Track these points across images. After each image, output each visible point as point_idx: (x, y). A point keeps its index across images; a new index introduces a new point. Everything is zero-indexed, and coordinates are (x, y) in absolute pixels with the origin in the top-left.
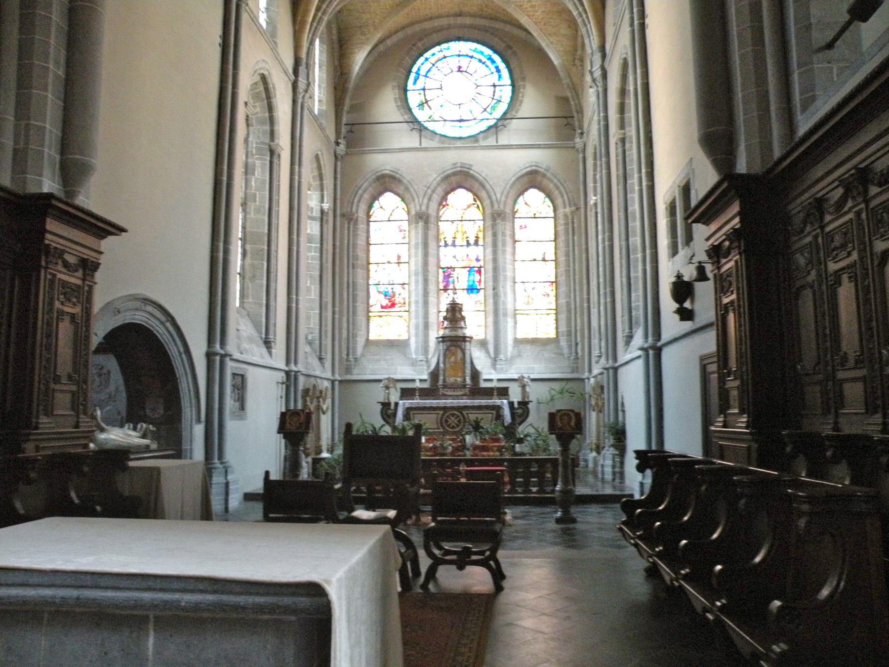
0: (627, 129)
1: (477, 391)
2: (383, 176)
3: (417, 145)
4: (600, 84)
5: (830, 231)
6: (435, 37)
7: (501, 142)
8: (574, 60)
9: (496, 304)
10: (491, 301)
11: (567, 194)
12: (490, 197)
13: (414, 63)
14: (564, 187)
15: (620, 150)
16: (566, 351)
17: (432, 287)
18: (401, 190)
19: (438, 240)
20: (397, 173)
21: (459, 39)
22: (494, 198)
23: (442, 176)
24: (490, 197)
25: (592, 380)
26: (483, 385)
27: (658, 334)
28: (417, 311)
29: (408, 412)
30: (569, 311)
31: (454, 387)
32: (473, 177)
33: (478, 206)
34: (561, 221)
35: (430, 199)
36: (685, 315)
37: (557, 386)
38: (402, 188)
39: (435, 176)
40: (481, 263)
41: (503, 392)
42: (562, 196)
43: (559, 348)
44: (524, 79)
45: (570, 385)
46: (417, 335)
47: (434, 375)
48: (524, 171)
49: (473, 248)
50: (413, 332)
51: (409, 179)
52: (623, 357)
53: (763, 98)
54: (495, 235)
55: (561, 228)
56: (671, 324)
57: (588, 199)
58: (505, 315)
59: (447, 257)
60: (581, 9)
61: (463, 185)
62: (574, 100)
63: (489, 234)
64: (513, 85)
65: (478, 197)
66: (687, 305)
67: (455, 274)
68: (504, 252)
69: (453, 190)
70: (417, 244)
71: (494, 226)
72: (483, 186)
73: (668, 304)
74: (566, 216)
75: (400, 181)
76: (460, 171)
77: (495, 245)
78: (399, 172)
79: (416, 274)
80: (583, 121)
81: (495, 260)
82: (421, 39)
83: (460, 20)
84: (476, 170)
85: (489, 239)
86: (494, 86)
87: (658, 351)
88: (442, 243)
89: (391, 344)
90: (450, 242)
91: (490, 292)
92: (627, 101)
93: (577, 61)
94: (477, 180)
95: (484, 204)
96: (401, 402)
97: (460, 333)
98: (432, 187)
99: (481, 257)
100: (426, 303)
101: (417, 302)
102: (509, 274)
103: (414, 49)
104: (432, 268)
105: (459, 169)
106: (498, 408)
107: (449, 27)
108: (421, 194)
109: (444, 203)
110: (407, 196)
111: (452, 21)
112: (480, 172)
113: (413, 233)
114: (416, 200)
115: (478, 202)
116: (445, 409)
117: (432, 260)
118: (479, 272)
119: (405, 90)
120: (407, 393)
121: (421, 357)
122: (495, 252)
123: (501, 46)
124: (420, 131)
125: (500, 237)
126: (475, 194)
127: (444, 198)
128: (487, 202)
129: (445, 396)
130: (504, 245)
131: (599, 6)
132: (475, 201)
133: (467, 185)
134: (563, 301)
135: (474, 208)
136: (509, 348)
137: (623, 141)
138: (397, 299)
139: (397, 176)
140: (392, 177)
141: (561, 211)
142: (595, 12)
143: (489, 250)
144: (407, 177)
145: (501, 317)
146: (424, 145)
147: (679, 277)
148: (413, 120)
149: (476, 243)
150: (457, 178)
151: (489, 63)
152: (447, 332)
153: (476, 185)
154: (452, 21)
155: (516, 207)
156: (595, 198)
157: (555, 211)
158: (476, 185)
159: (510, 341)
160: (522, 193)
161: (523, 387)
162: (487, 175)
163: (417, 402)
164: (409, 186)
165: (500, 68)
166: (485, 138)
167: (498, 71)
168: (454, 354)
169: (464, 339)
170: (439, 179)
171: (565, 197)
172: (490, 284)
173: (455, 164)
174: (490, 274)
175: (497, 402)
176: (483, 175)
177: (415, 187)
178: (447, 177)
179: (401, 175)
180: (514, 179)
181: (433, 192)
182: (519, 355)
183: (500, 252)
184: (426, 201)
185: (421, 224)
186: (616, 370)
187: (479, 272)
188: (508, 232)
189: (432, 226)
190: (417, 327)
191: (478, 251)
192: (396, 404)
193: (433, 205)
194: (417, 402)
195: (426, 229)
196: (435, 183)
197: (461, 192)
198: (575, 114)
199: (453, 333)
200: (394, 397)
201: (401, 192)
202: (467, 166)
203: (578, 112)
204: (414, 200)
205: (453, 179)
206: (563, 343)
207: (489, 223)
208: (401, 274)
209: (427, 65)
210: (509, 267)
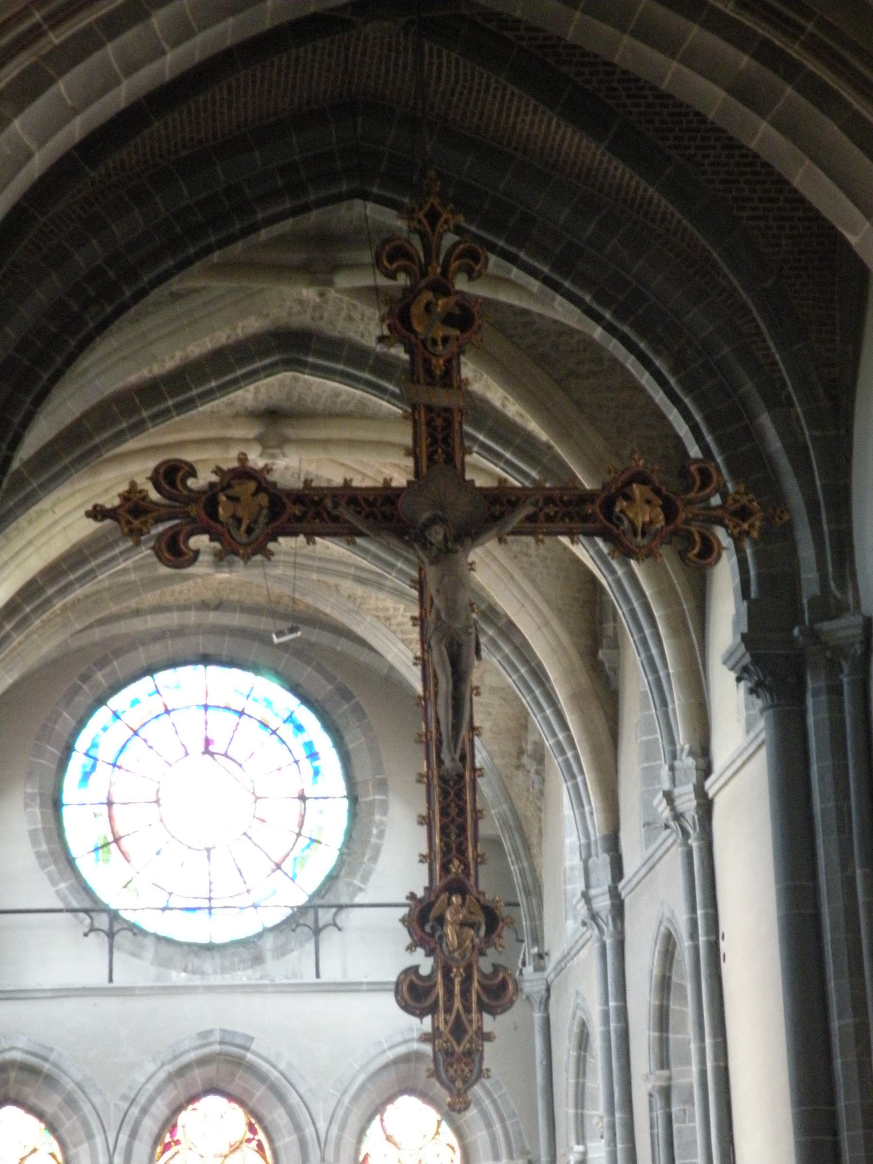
0: (675, 1068)
3: (101, 980)
4: (609, 929)
6: (141, 656)
7: (331, 973)
8: (521, 752)
11: (502, 1120)
12: (298, 1128)
13: (81, 723)
14: (494, 1102)
15: (659, 1113)
18: (51, 1104)
20: (46, 1059)
21: (206, 659)
22: (309, 1131)
23: (170, 1068)
24: (298, 1128)
32: (252, 1069)
33: (260, 1146)
35: (133, 1134)
38: (57, 1099)
39: (150, 1067)
42: (489, 1125)
44: (382, 785)
48: (391, 1055)
51: (78, 1077)
57: (560, 1151)
60: (561, 736)
61: (222, 1085)
62: (518, 858)
64: (353, 798)
65: (260, 1120)
69: (193, 1099)
72: (281, 1098)
75: (50, 1081)
76: (220, 1054)
78: (53, 1057)
80: (541, 918)
82: (103, 663)
83: (212, 617)
84: (260, 1051)
86: (302, 798)
92: (674, 1006)
93: (525, 760)
94: (263, 1078)
95: (279, 1144)
98: (142, 1100)
103: (86, 687)
105: (217, 1048)
107: (180, 632)
109: (167, 1139)
110: (69, 1123)
111: (192, 617)
112: (272, 1058)
114: (99, 1140)
115: (261, 1136)
119: (57, 804)
123: (323, 689)
124: (111, 935)
126: (251, 1112)
127: (169, 1124)
128: (287, 1140)
131: (604, 738)
132: (252, 1129)
133: (231, 1089)
135: (249, 1151)
137: (666, 1093)
139: (47, 1067)
140: (32, 1071)
142: (596, 752)
146: (119, 980)
148: (87, 904)
150: (210, 1071)
151: (286, 731)
154: (192, 617)
155: (364, 1149)
156: (580, 1148)
158: (260, 1091)
160: (378, 1109)
162: (290, 1065)
164: (78, 1095)
165: (317, 748)
166: (281, 952)
167: (313, 756)
170: (162, 1075)
171: (498, 1127)
173: (205, 1034)
176: (282, 1066)
177: (97, 1100)
178: (182, 1071)
179: (56, 1065)
180: (362, 1077)
181: (144, 1111)
184: (124, 1138)
196: (150, 1087)
197: (213, 1103)
198: (521, 899)
201: (49, 1109)
202: (238, 1041)
203: (527, 893)
204: (90, 1136)
205: (198, 1075)
209: (119, 733)
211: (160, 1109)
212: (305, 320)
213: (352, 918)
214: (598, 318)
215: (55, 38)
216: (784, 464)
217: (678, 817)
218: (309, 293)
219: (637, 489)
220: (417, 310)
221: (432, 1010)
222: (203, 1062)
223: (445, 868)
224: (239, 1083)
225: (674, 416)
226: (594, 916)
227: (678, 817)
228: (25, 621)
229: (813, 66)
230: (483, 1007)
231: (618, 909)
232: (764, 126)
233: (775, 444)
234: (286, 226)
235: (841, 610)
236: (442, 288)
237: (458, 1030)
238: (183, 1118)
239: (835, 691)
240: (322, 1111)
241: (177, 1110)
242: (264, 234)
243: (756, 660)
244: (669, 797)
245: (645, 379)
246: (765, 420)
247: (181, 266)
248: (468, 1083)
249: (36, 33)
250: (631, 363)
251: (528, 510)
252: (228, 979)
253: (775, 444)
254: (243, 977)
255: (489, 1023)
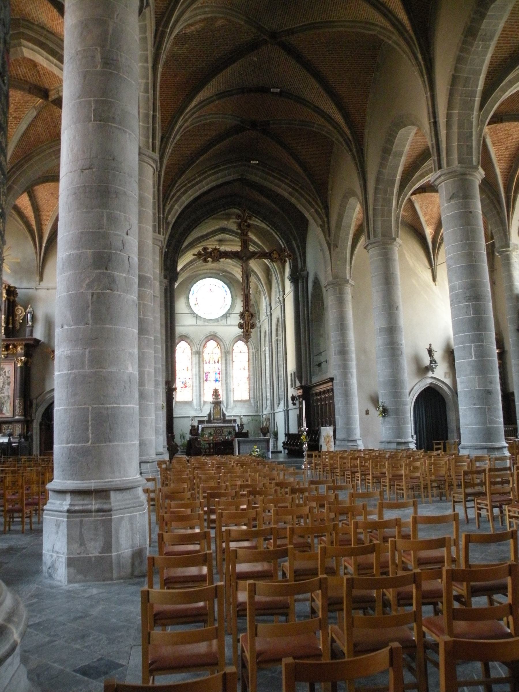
1: (225, 421)
2: (182, 336)
3: (195, 324)
5: (320, 393)
6: (201, 277)
7: (229, 323)
9: (227, 387)
10: (224, 386)
12: (224, 345)
16: (253, 405)
17: (202, 380)
18: (189, 341)
19: (203, 361)
21: (210, 277)
24: (224, 345)
25: (264, 416)
26: (227, 418)
27: (288, 406)
28: (196, 390)
29: (203, 429)
30: (254, 390)
31: (217, 419)
32: (217, 337)
34: (251, 355)
35: (200, 345)
36: (294, 404)
37: (250, 418)
40: (220, 370)
41: (235, 421)
43: (250, 403)
44: (236, 296)
45: (255, 417)
46: (196, 399)
47: (210, 415)
49: (217, 364)
50: (194, 398)
52: (277, 410)
53: (307, 371)
54: (226, 360)
55: (251, 357)
56: (291, 405)
58: (230, 391)
59: (207, 368)
63: (224, 359)
64: (232, 298)
66: (295, 402)
67: (209, 375)
68: (230, 367)
70: (196, 363)
71: (226, 356)
73: (290, 402)
74: (253, 353)
75: (188, 338)
77: (226, 363)
79: (196, 375)
81: (226, 370)
82: (195, 277)
83: (211, 271)
85: (224, 361)
87: (288, 411)
88: (205, 362)
89: (186, 403)
90: (207, 362)
91: (224, 382)
92: (279, 328)
94: (219, 338)
96: (200, 426)
97: (219, 400)
99: (220, 368)
100: (200, 387)
101: (196, 386)
102: (231, 375)
104: (202, 372)
106: (234, 427)
107: (206, 273)
108: (197, 343)
110: (191, 344)
111: (208, 271)
113: (194, 358)
116: (216, 427)
117: (201, 369)
118: (219, 374)
119: (188, 298)
120: (200, 422)
121: (198, 408)
122: (226, 367)
123: (228, 282)
125: (228, 361)
126: (217, 343)
127: (205, 344)
128: (222, 347)
129: (214, 423)
130: (230, 364)
134: (252, 385)
136: (232, 404)
138: (187, 385)
141: (251, 350)
142: (268, 291)
143: (224, 366)
144: (192, 336)
145: (229, 392)
146: (198, 324)
147: (293, 395)
149: (218, 362)
152: (214, 400)
153: (218, 340)
154: (208, 271)
157: (248, 349)
159: (232, 401)
160: (235, 343)
161: (241, 419)
163: (205, 425)
166: (222, 320)
168: (217, 408)
169: (220, 402)
172: (224, 379)
173: (210, 332)
174: (224, 375)
175: (233, 424)
178: (207, 337)
182: (236, 406)
183: (228, 367)
185: (197, 355)
186: (274, 414)
187: (219, 374)
188: (231, 359)
189: (201, 356)
190: (196, 396)
191: (219, 365)
192: (198, 427)
193: (202, 347)
194: (205, 425)
195: (199, 357)
197: (212, 341)
199: (216, 401)
200: (196, 424)
205: (210, 338)
206: (252, 401)
207: (223, 355)
208: (189, 374)
210: (231, 372)
211: (204, 342)
212: (225, 226)
213: (232, 315)
214: (269, 227)
215: (189, 185)
216: (296, 249)
217: (280, 301)
218: (226, 222)
219: (275, 252)
220: (242, 224)
221: (243, 328)
222: (210, 336)
223: (245, 308)
224: (215, 338)
225: (280, 241)
226: (267, 315)
227: (280, 301)
228: (184, 271)
229: (300, 190)
230: (251, 328)
231: (271, 314)
232: (293, 199)
233: (295, 246)
234: (223, 212)
235: (304, 271)
236: (246, 221)
237: (247, 331)
238: (208, 344)
239: (303, 282)
240: (227, 343)
241: (207, 342)
242: (220, 213)
243: (292, 278)
244: (279, 298)
245: (276, 236)
246: (294, 242)
247: (207, 218)
248: (248, 339)
249: (186, 185)
250: (274, 234)
251: (258, 255)
252: (214, 324)
253: (295, 246)
254: (216, 324)
255: (252, 330)
